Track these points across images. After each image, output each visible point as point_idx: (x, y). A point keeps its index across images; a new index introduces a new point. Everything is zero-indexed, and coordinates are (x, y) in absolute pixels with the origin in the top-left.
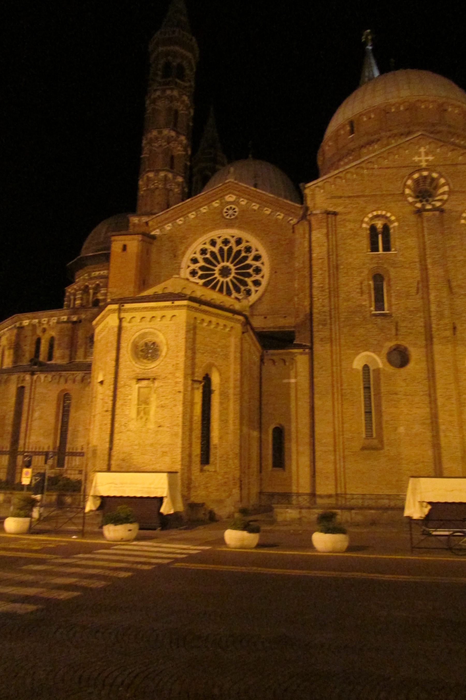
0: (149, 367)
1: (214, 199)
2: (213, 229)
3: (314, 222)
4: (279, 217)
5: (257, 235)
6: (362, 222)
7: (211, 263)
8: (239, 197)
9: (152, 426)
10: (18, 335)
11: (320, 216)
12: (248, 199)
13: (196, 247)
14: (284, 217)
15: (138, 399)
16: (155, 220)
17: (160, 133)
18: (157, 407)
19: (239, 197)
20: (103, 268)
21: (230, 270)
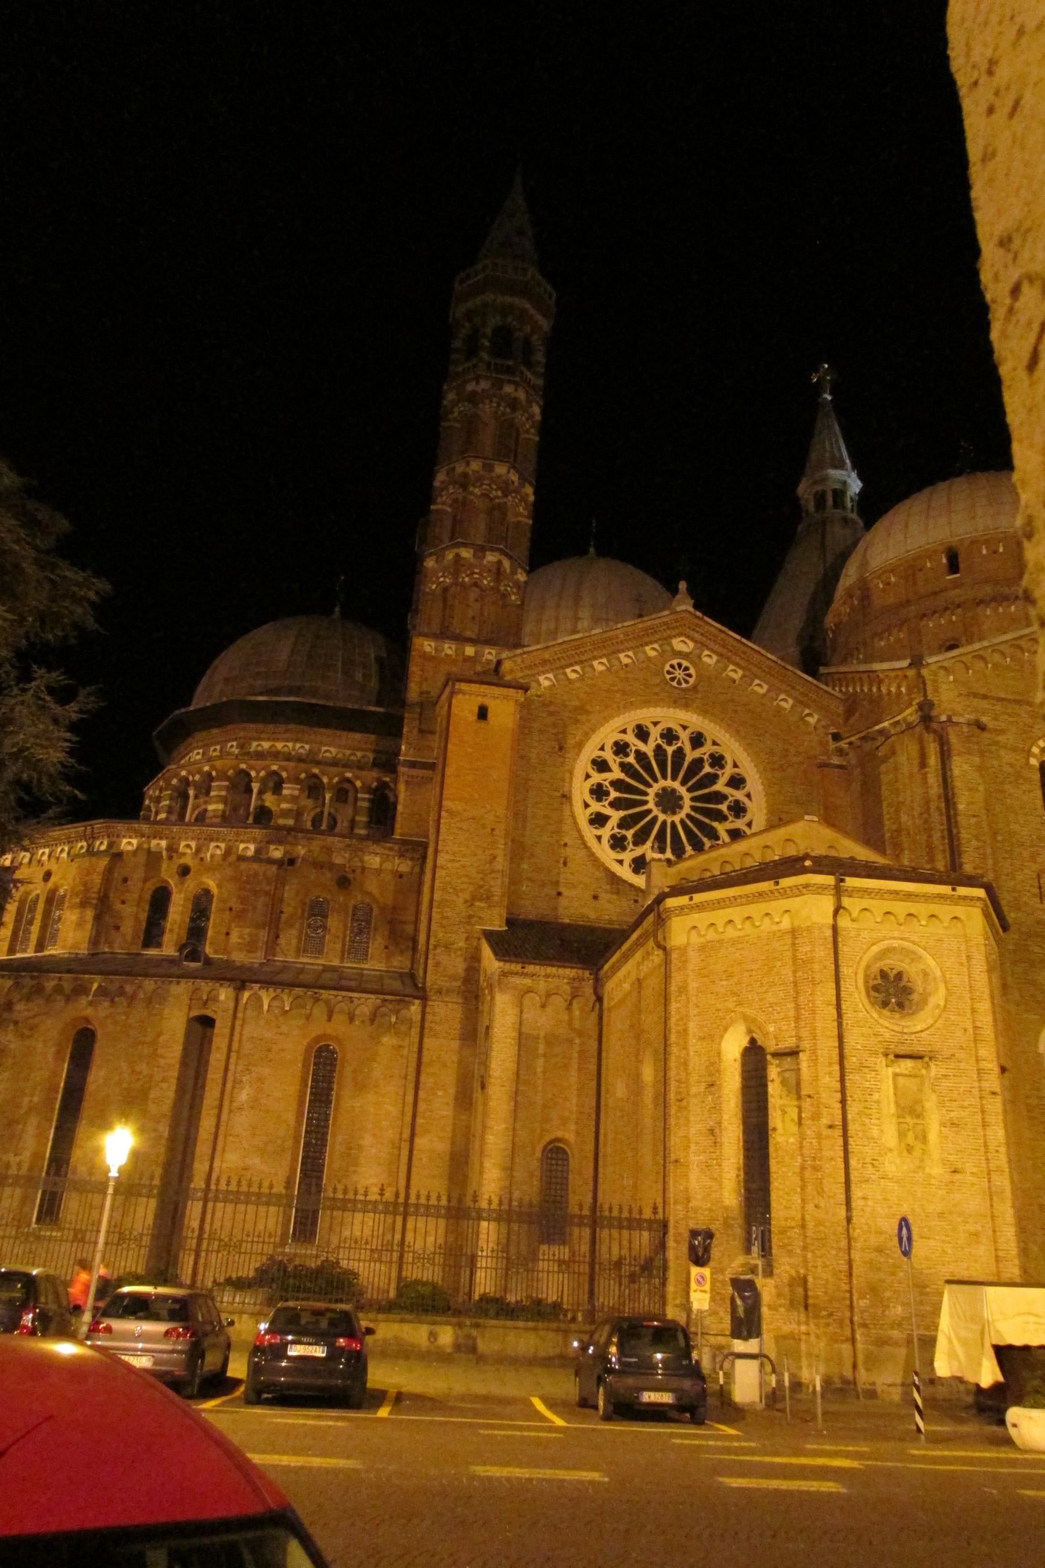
0: (914, 1030)
1: (647, 639)
2: (647, 703)
3: (953, 739)
4: (783, 704)
5: (737, 733)
6: (1029, 753)
7: (635, 775)
8: (701, 645)
9: (936, 1170)
10: (108, 874)
11: (965, 729)
12: (720, 655)
13: (606, 737)
14: (792, 707)
15: (896, 1102)
16: (519, 660)
17: (489, 468)
18: (943, 1124)
19: (701, 645)
20: (286, 736)
21: (681, 798)
